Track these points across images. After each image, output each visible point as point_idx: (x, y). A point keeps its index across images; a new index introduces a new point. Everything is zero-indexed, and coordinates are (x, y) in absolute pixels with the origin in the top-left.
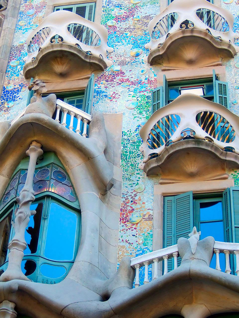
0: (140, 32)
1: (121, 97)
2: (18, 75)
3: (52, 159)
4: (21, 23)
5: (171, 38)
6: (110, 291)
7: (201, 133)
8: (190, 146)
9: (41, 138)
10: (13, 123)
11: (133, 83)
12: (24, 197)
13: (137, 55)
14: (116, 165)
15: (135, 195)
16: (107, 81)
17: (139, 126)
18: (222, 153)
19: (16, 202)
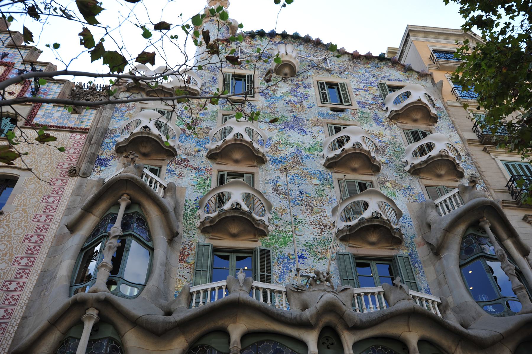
0: (202, 137)
1: (186, 177)
2: (110, 149)
3: (136, 209)
5: (226, 142)
6: (172, 310)
7: (245, 208)
8: (236, 214)
9: (131, 192)
10: (106, 181)
11: (194, 168)
12: (114, 232)
13: (199, 151)
14: (179, 221)
15: (192, 244)
16: (177, 164)
17: (197, 198)
18: (256, 223)
19: (107, 236)
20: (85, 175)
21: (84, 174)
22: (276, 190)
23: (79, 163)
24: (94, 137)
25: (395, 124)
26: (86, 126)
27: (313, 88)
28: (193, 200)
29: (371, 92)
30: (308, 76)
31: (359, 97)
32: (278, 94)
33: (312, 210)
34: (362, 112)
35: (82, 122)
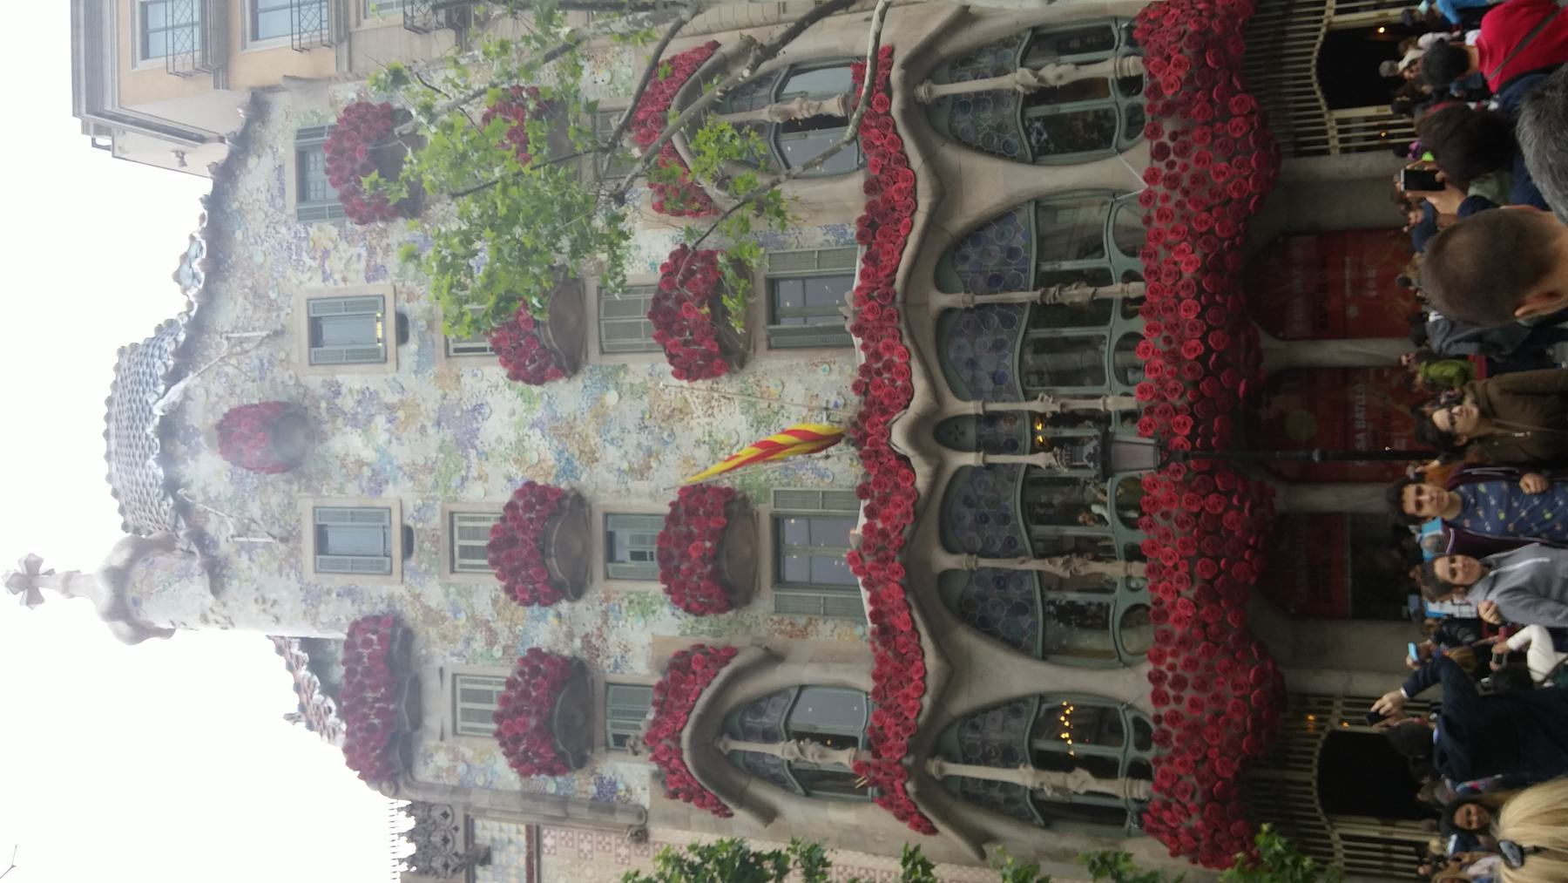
4: (480, 781)
11: (605, 622)
12: (791, 753)
20: (642, 813)
21: (640, 816)
22: (642, 472)
23: (617, 829)
24: (549, 812)
25: (428, 208)
26: (519, 832)
27: (340, 378)
28: (677, 621)
29: (330, 246)
30: (298, 384)
31: (351, 276)
32: (369, 455)
33: (681, 411)
34: (400, 275)
35: (510, 841)
